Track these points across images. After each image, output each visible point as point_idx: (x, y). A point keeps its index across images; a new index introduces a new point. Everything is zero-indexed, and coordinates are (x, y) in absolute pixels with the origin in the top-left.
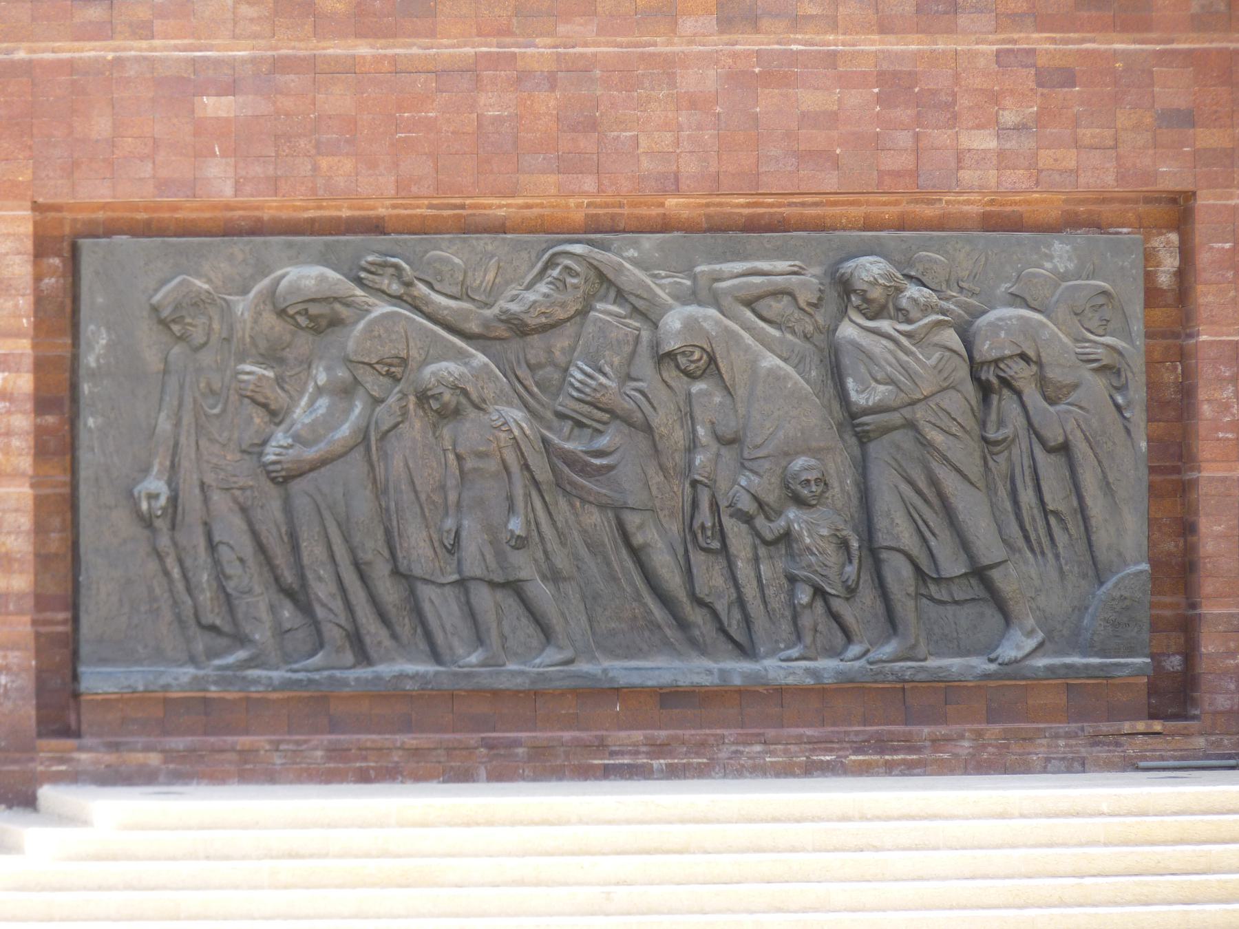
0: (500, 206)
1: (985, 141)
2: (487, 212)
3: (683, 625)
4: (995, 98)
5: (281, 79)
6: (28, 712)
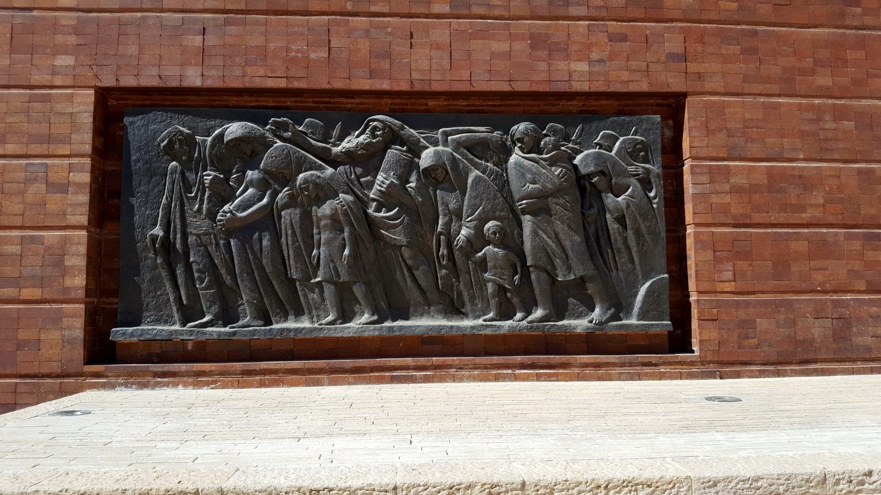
0: (348, 103)
1: (583, 67)
4: (589, 47)
5: (228, 28)
6: (79, 352)
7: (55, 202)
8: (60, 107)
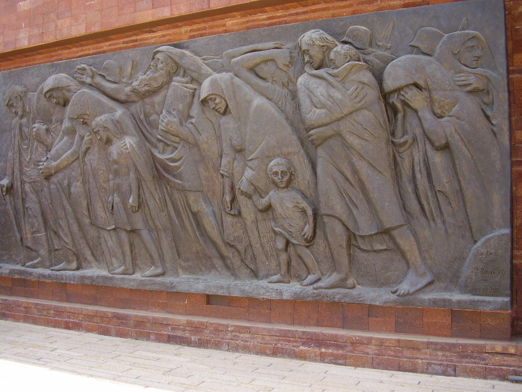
0: (152, 38)
2: (146, 42)
3: (223, 258)
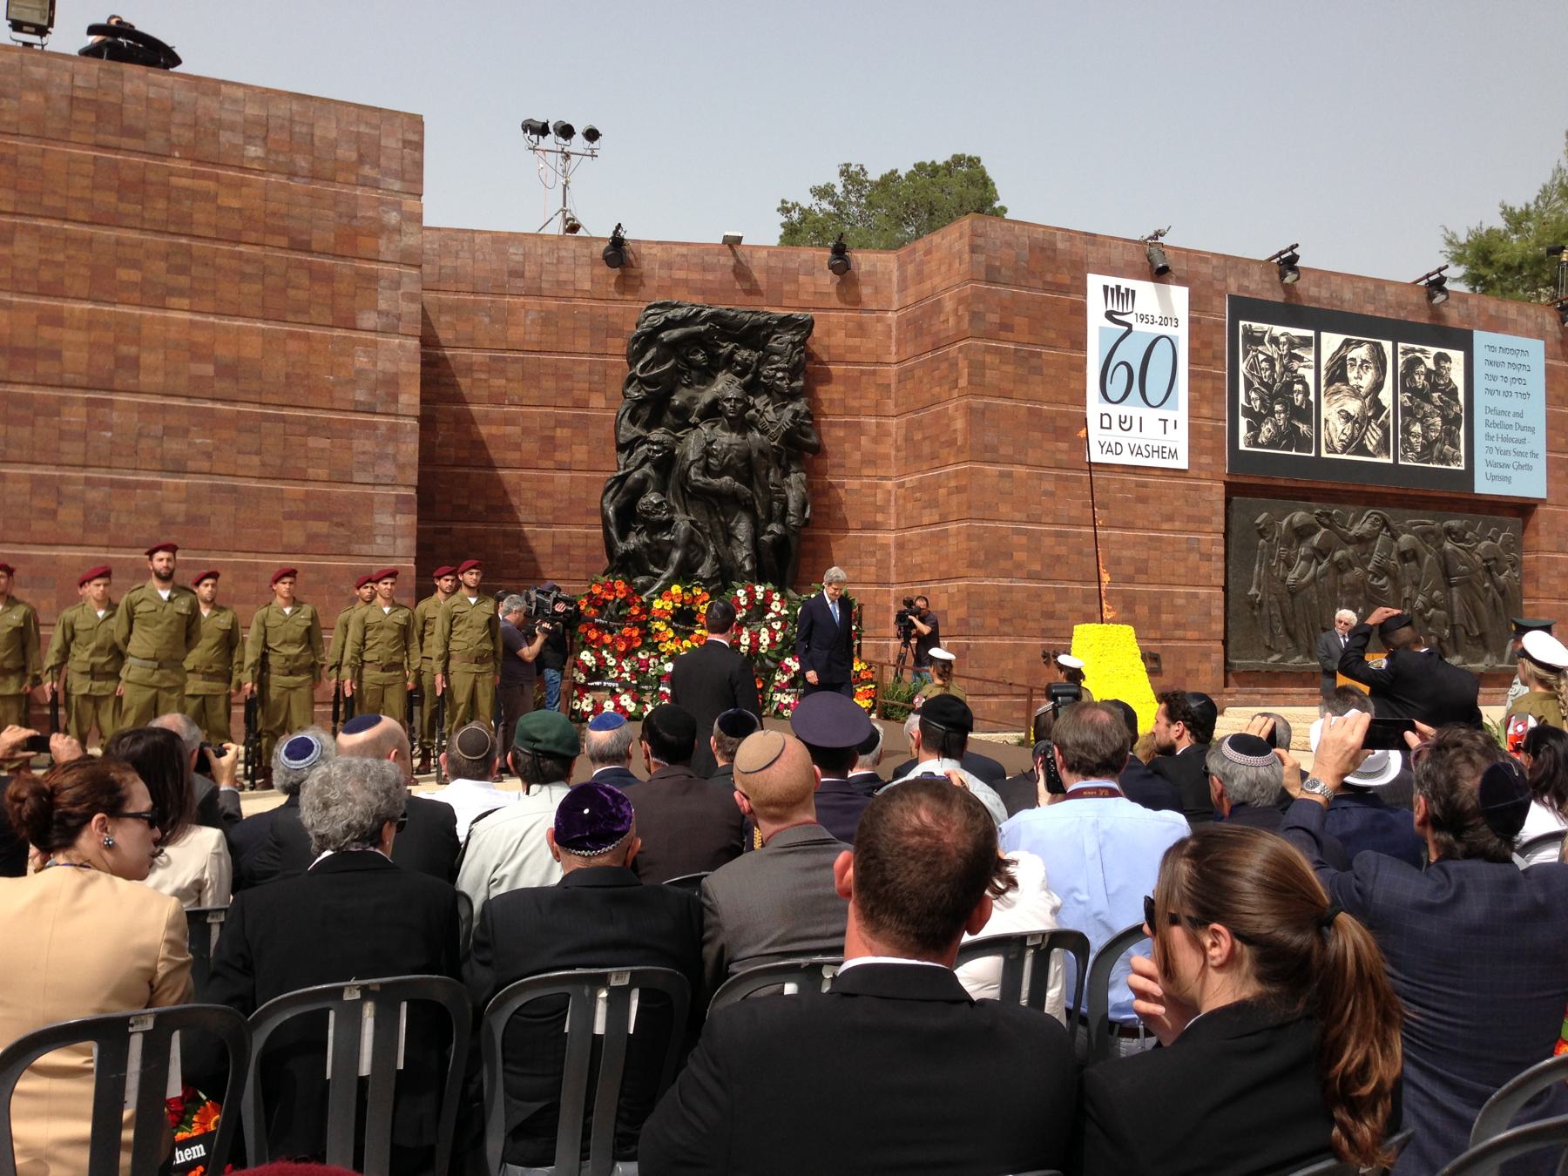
7: (1205, 567)
8: (1206, 495)
